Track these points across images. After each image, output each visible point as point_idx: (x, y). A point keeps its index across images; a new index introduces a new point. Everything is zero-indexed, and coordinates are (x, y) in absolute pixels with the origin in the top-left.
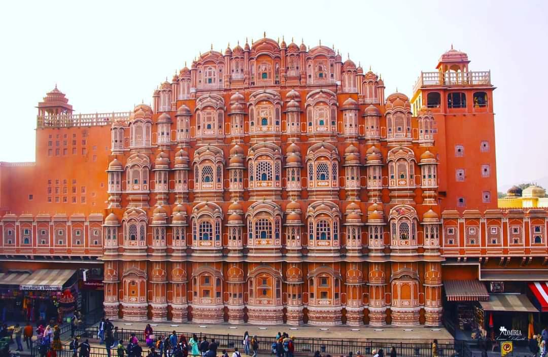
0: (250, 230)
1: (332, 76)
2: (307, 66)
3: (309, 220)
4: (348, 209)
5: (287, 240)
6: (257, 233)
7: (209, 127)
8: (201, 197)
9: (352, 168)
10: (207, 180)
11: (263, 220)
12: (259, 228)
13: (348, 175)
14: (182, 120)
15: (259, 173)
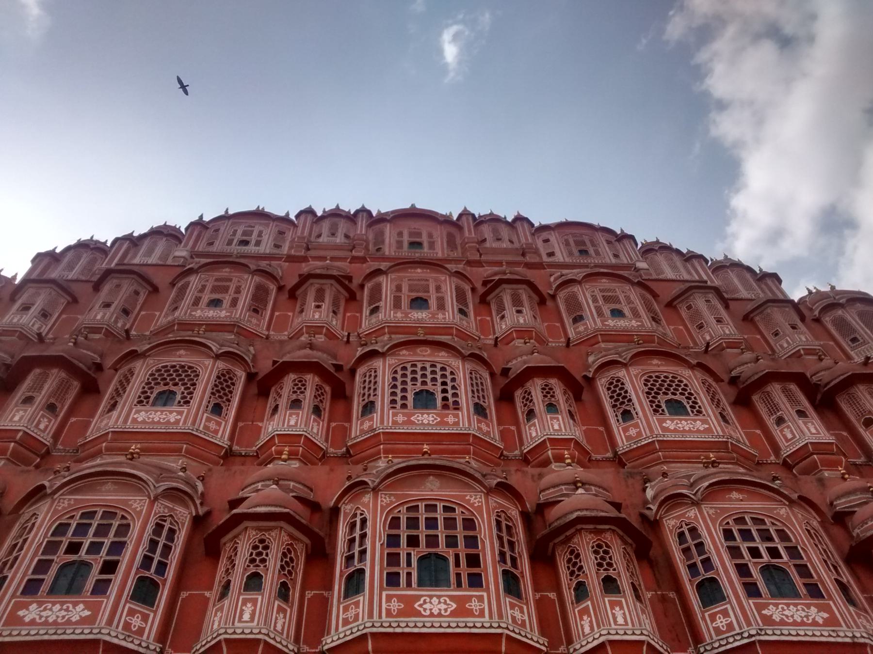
0: (350, 559)
1: (616, 256)
2: (540, 243)
3: (670, 523)
4: (839, 497)
5: (573, 611)
6: (393, 559)
7: (215, 303)
8: (107, 449)
9: (785, 391)
10: (165, 398)
11: (431, 508)
12: (403, 541)
13: (774, 409)
14: (118, 286)
15: (404, 390)
